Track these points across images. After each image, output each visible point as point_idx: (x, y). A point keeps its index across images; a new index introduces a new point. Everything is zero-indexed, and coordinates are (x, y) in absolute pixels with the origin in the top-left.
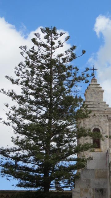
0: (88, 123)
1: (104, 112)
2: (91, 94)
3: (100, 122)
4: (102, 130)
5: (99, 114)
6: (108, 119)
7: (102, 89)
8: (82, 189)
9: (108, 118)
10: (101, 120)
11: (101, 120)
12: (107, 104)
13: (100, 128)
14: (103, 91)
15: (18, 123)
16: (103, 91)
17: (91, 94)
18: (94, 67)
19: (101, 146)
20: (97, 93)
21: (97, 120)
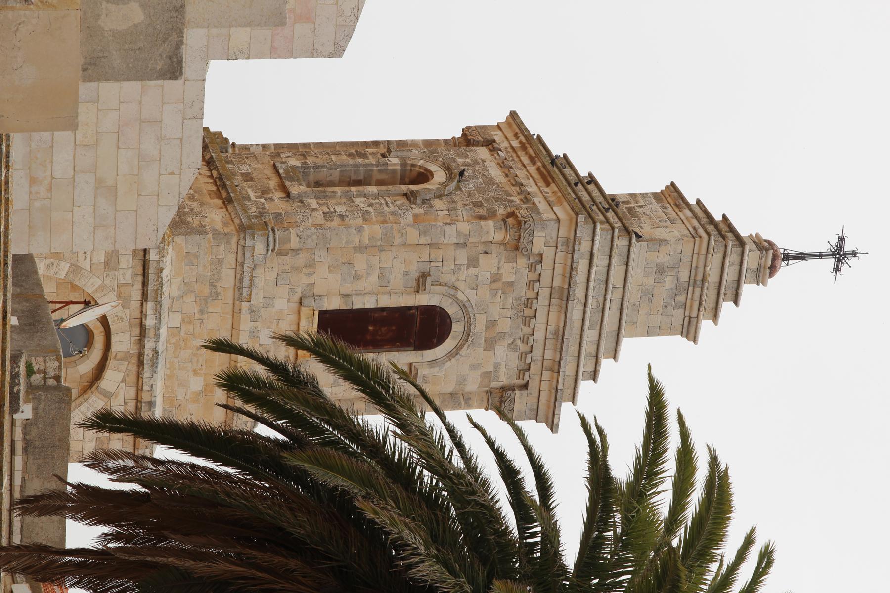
0: (488, 275)
1: (552, 370)
2: (676, 267)
3: (490, 345)
4: (433, 363)
5: (539, 335)
6: (503, 389)
7: (706, 325)
9: (512, 389)
12: (606, 364)
13: (449, 344)
14: (690, 331)
16: (690, 331)
17: (676, 267)
18: (854, 254)
20: (681, 298)
21: (505, 325)
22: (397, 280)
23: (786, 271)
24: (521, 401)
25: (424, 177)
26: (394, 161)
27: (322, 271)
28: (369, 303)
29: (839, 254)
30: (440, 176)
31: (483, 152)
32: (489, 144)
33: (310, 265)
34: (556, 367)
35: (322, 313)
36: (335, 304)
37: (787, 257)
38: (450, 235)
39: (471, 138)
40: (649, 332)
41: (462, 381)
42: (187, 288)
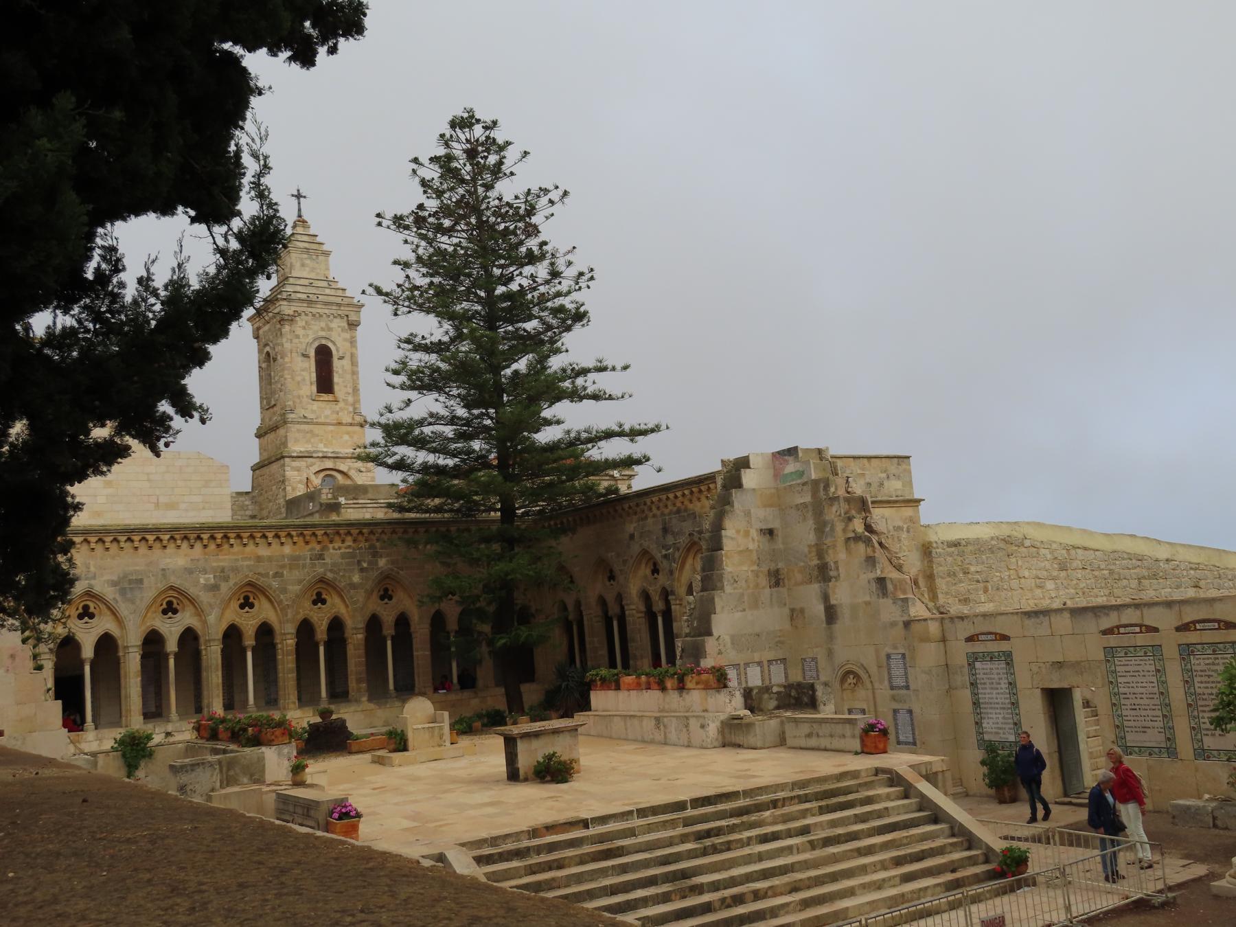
3: (330, 329)
7: (325, 248)
8: (738, 532)
10: (333, 325)
11: (333, 325)
13: (330, 345)
14: (327, 254)
15: (104, 322)
19: (336, 388)
21: (323, 324)
22: (306, 365)
23: (305, 217)
24: (353, 317)
25: (268, 354)
26: (264, 365)
27: (301, 393)
28: (314, 375)
29: (299, 196)
30: (268, 349)
31: (261, 332)
32: (258, 329)
33: (299, 397)
34: (339, 305)
35: (318, 392)
36: (314, 388)
37: (300, 216)
38: (287, 345)
39: (257, 337)
40: (328, 269)
41: (345, 340)
42: (308, 441)
